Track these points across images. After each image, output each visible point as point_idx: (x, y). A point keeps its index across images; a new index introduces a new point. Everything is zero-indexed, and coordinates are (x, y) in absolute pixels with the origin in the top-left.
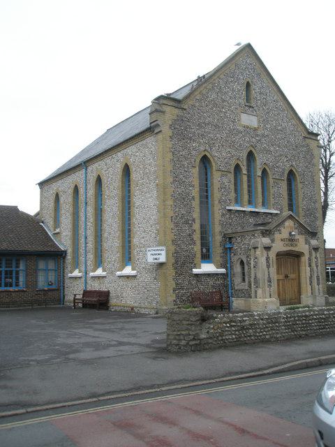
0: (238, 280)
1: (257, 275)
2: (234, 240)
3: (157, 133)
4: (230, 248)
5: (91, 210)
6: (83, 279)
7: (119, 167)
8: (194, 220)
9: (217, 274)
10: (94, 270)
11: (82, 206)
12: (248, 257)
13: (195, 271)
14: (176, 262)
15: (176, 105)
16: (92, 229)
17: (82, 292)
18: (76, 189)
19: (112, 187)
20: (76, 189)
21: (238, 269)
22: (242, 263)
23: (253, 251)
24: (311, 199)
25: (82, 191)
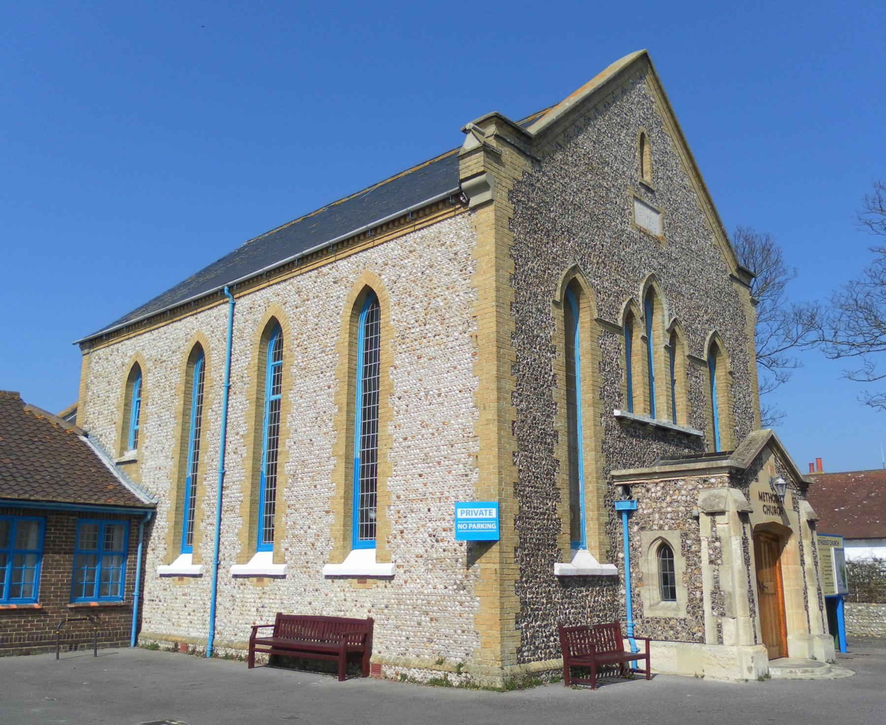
0: (651, 593)
1: (721, 584)
2: (636, 492)
3: (475, 209)
4: (630, 513)
5: (242, 406)
6: (207, 582)
7: (344, 298)
8: (555, 435)
9: (600, 578)
10: (245, 559)
11: (214, 395)
12: (685, 535)
13: (559, 569)
14: (522, 546)
15: (520, 145)
16: (246, 452)
17: (272, 621)
18: (197, 354)
19: (314, 348)
20: (197, 354)
21: (651, 565)
22: (665, 550)
23: (705, 520)
24: (745, 412)
25: (215, 359)
